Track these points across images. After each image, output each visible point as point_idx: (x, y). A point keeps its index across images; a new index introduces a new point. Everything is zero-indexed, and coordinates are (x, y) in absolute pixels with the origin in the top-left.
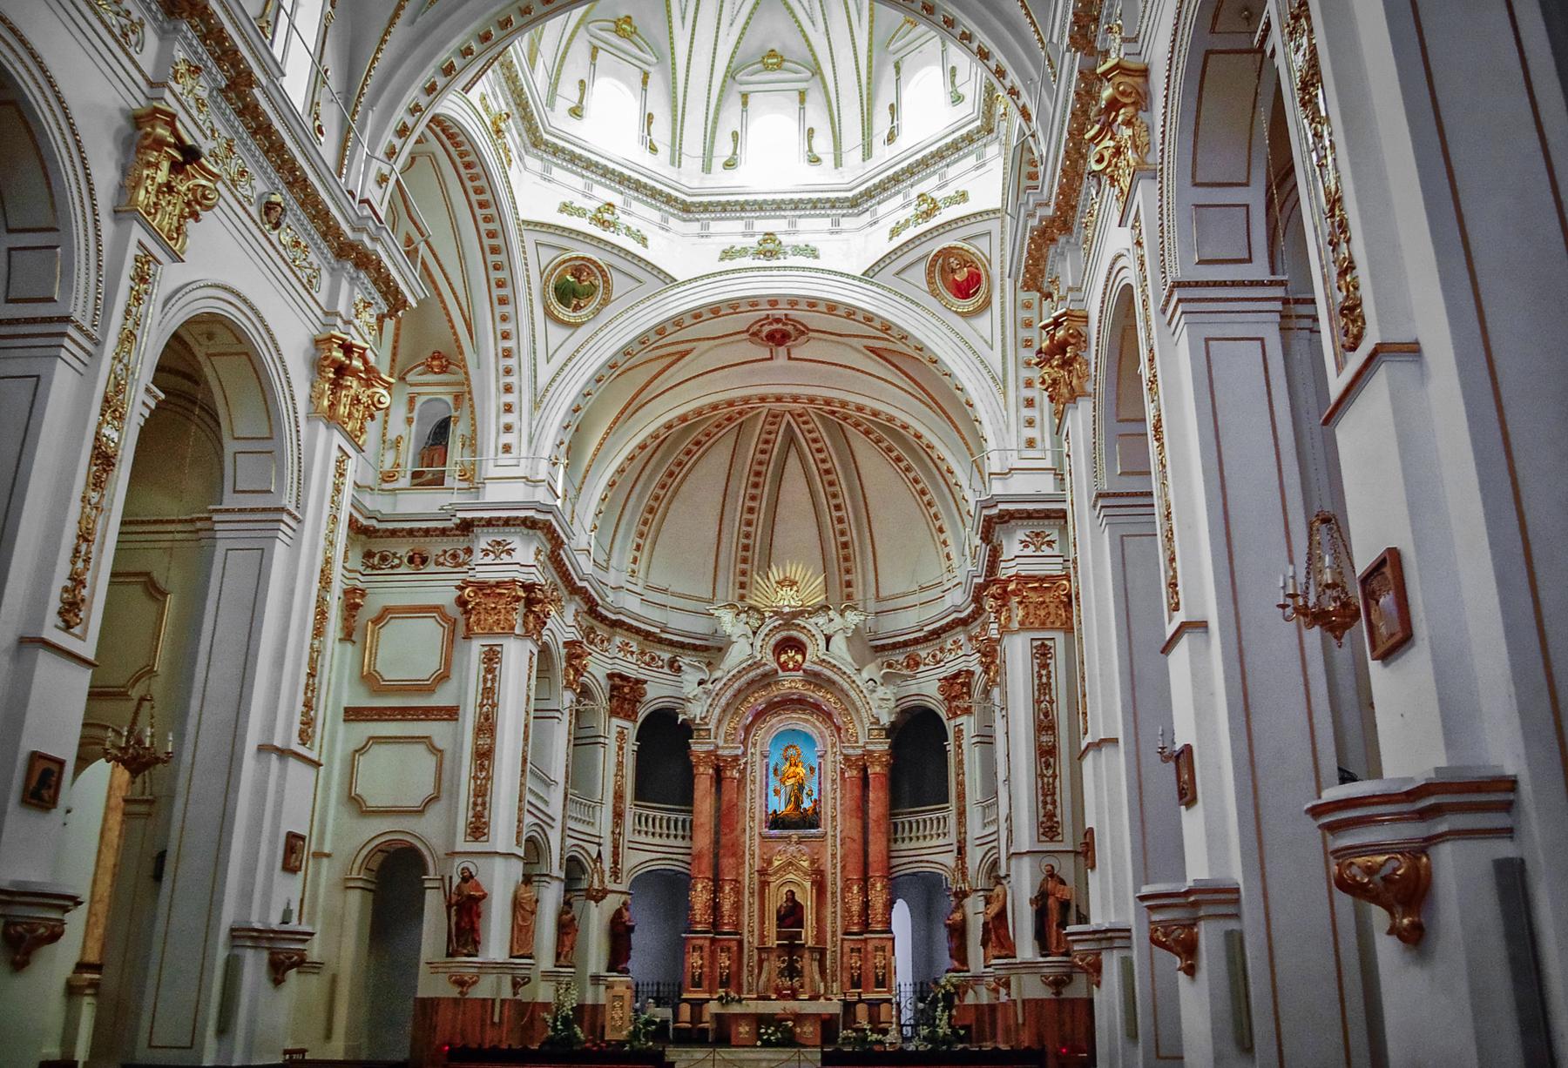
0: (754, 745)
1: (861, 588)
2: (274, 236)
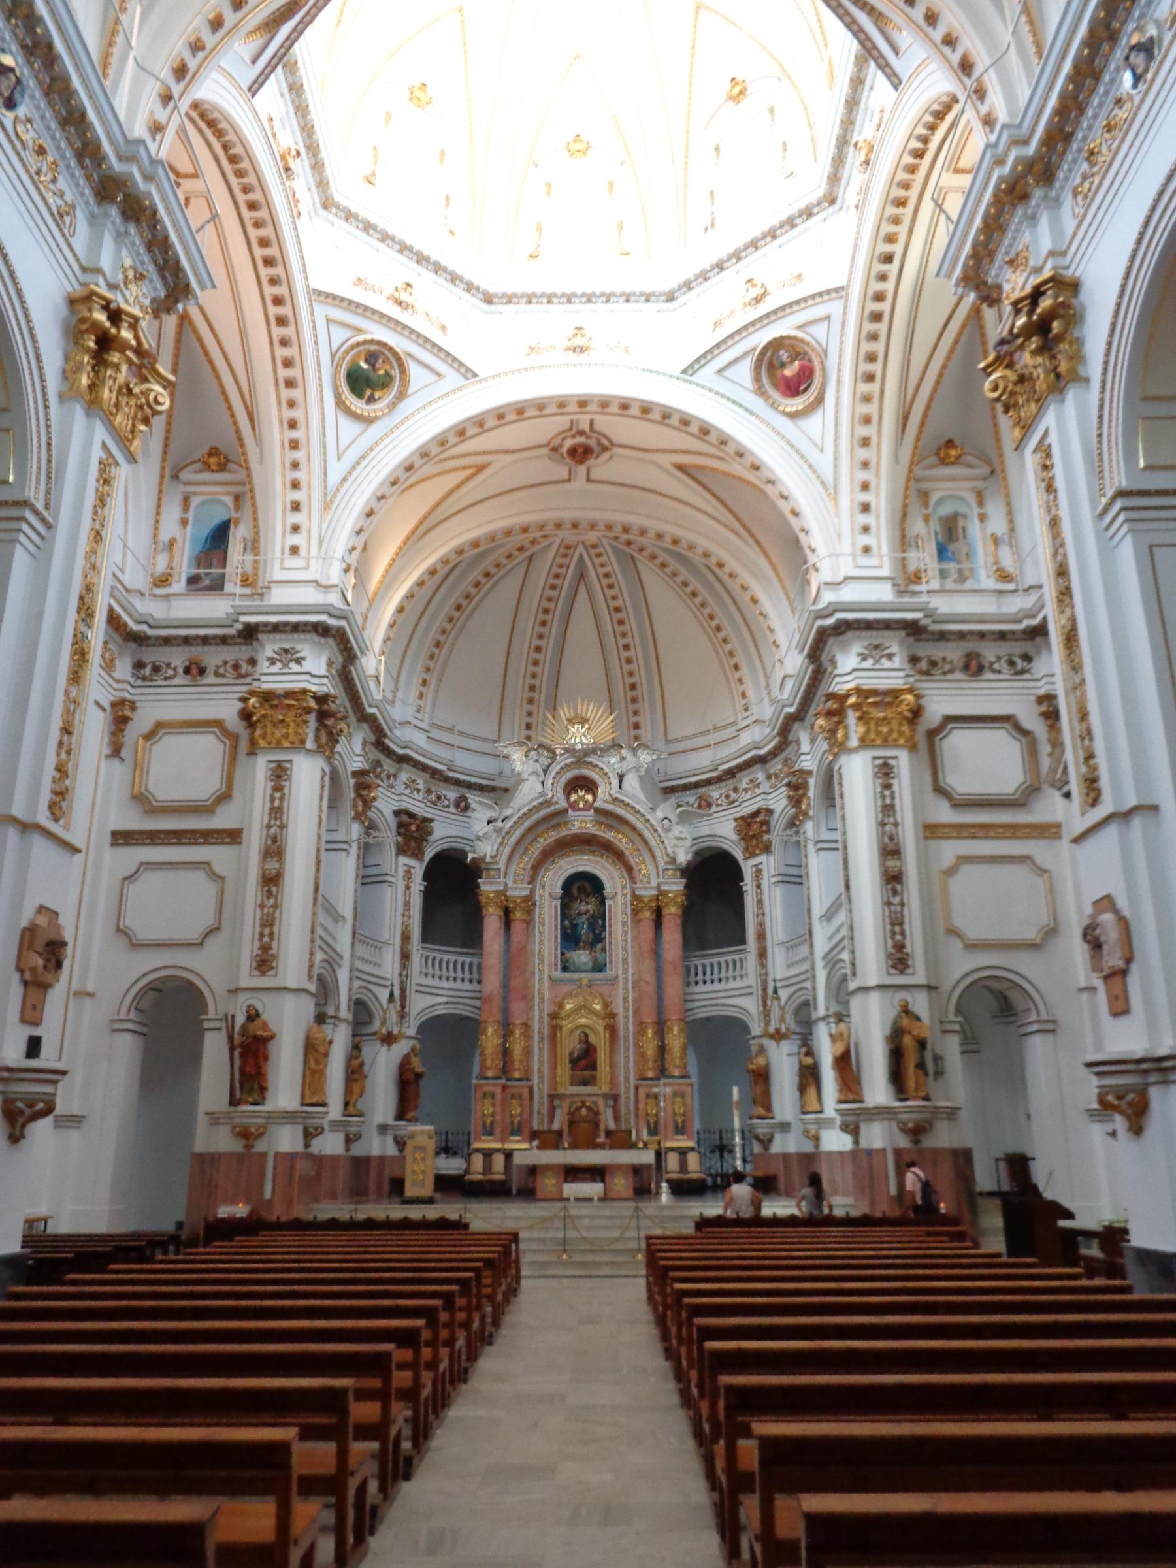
0: (543, 887)
1: (649, 729)
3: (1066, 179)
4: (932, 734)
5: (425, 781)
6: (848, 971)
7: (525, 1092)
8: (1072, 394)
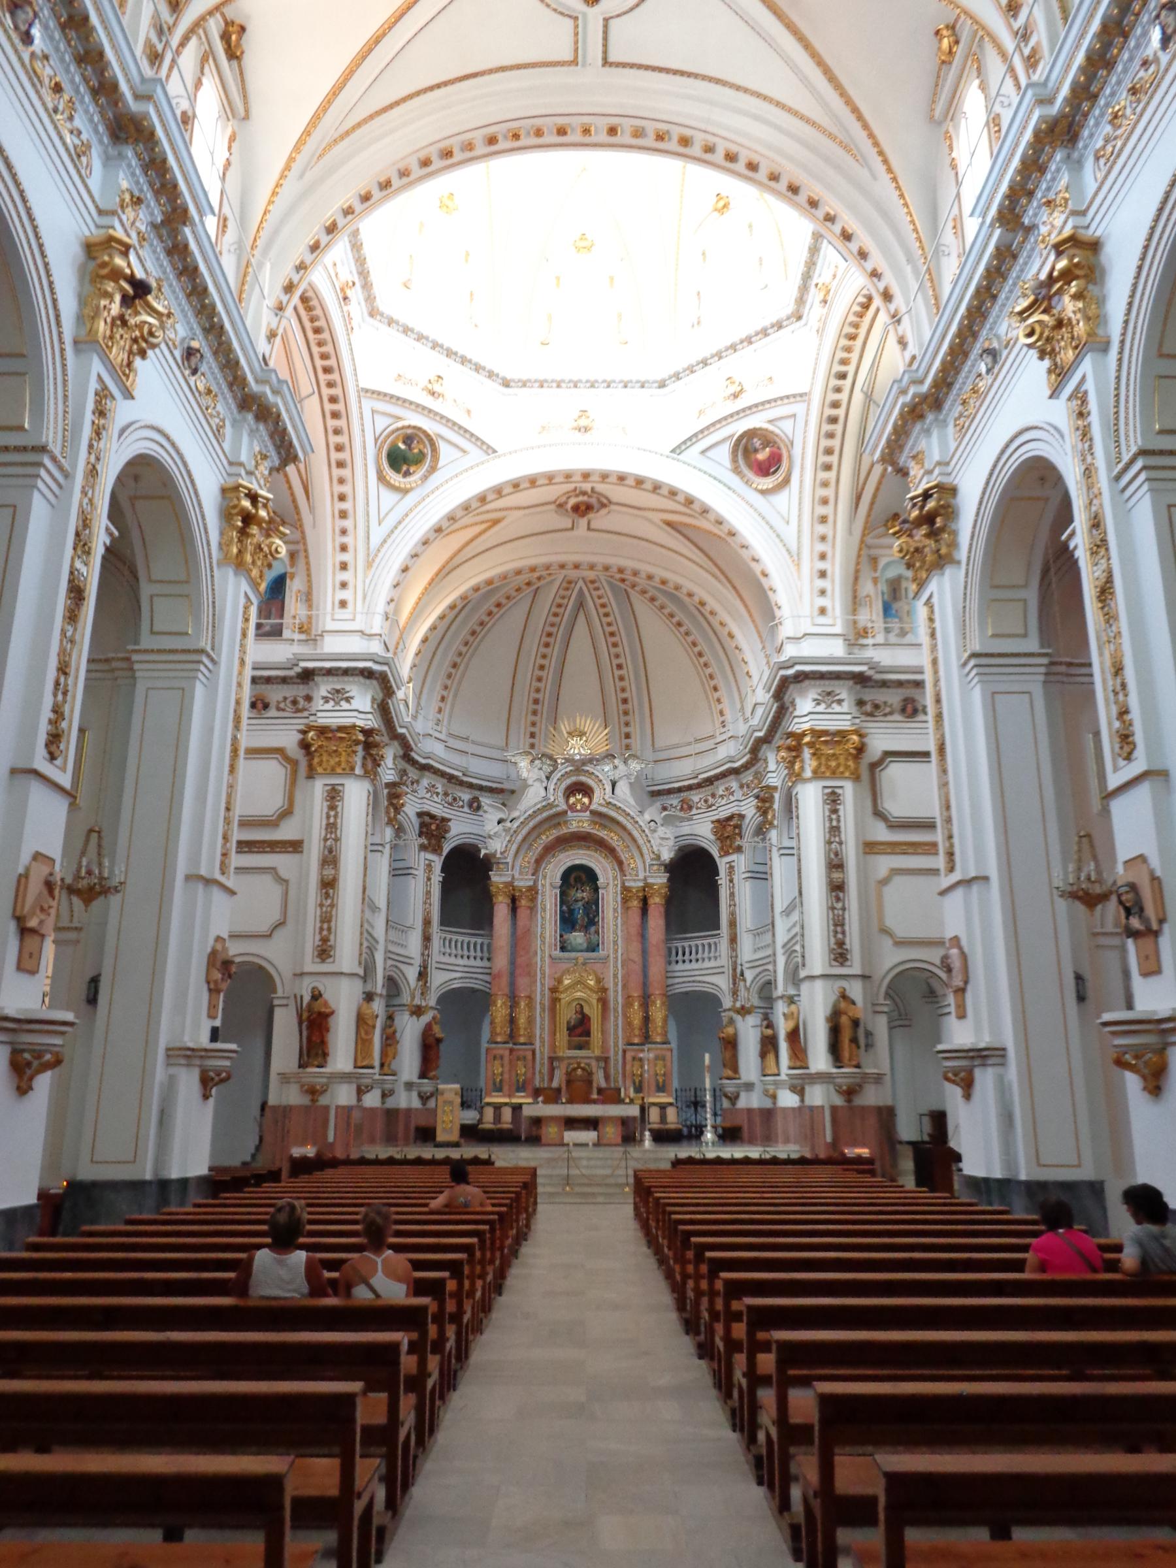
0: (545, 877)
2: (192, 380)
3: (950, 410)
4: (873, 766)
5: (443, 785)
6: (799, 960)
7: (529, 1055)
8: (949, 571)
